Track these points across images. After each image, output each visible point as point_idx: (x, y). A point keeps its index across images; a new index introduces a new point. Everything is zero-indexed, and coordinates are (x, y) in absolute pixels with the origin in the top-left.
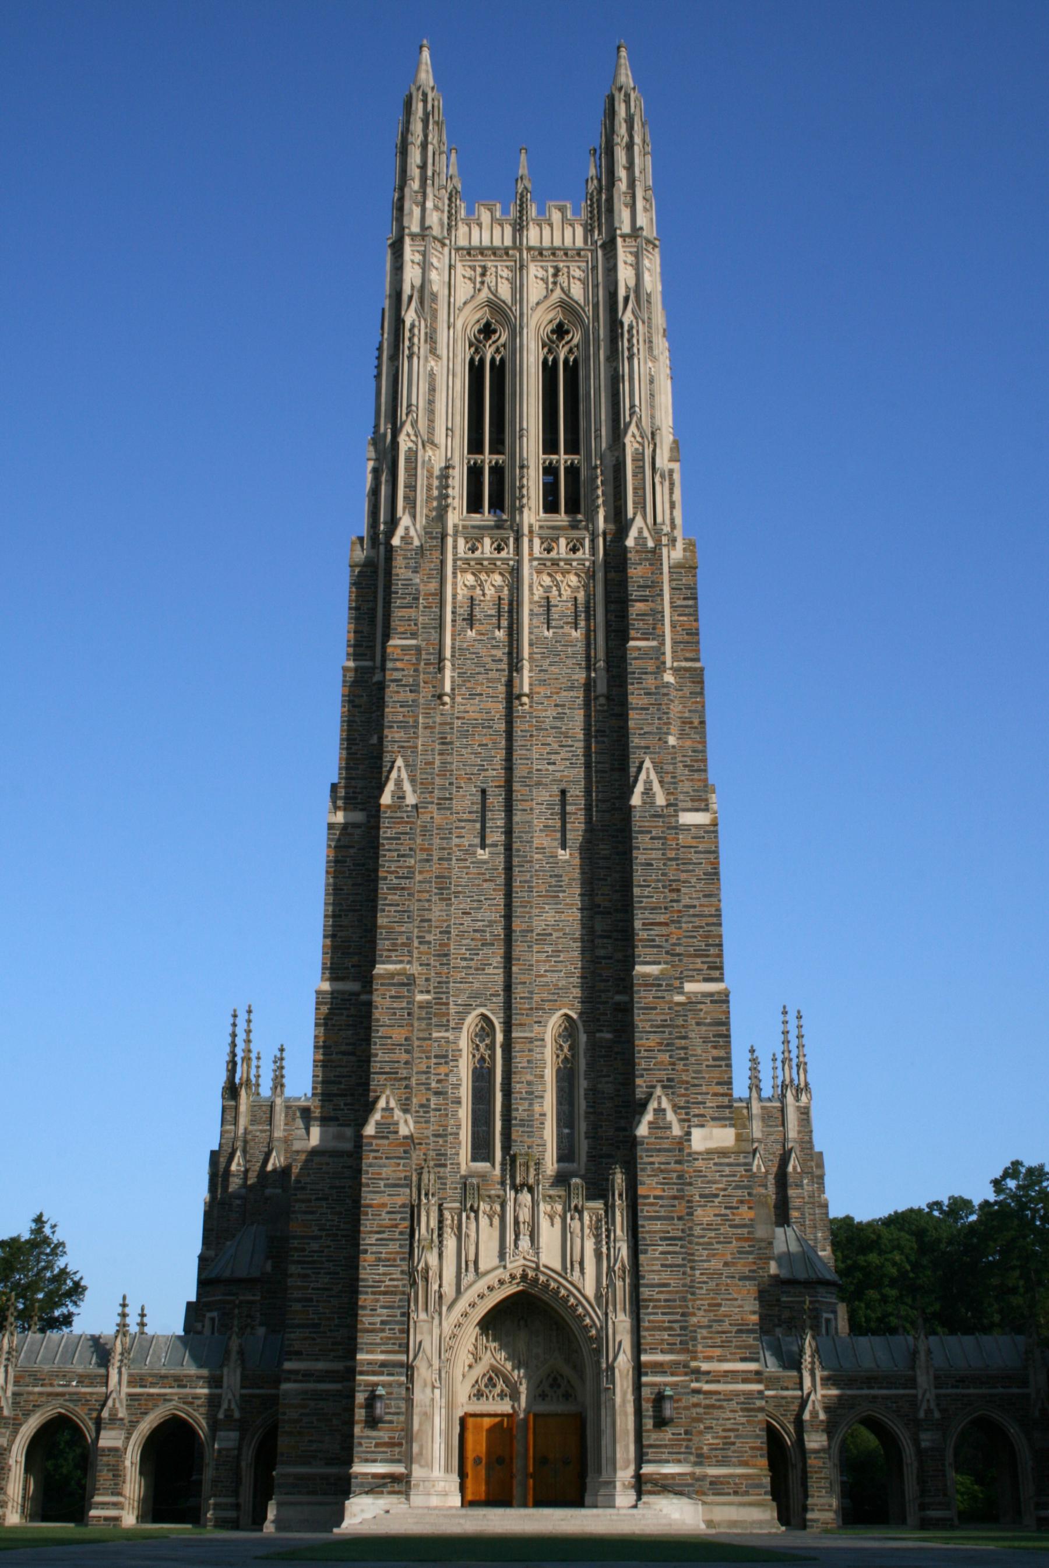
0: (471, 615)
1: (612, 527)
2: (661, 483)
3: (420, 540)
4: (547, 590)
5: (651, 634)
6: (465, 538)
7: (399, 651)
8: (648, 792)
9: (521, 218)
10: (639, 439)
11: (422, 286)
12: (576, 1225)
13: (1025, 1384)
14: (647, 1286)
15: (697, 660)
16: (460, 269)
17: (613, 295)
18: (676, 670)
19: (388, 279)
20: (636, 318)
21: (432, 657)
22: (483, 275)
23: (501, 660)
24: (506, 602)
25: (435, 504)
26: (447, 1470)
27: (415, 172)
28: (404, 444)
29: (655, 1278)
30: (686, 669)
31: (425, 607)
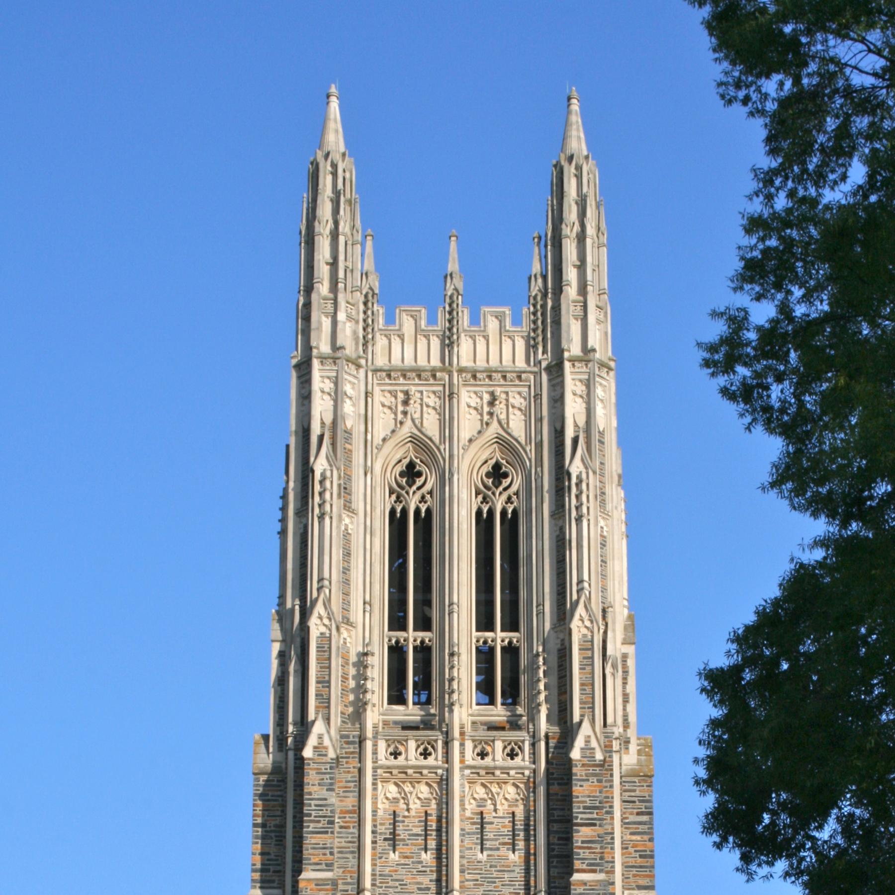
0: (394, 833)
1: (556, 729)
2: (613, 674)
3: (335, 751)
4: (481, 803)
5: (598, 865)
6: (387, 740)
7: (313, 886)
9: (450, 329)
10: (588, 623)
11: (334, 423)
16: (378, 397)
17: (558, 433)
19: (293, 411)
20: (586, 468)
21: (349, 887)
22: (406, 403)
23: (428, 889)
24: (434, 818)
25: (351, 697)
27: (323, 271)
28: (316, 628)
31: (341, 827)
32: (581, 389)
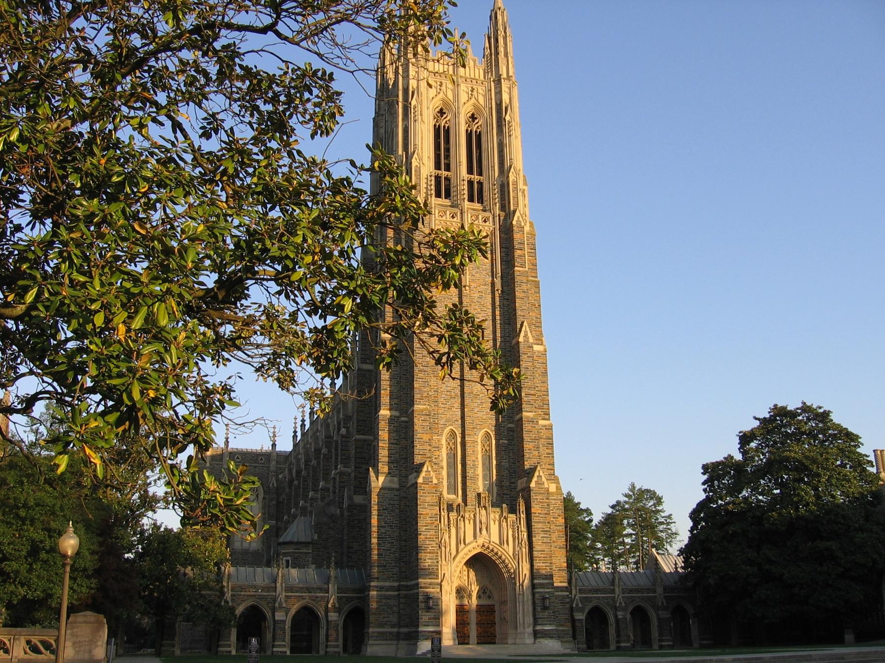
8: (526, 336)
12: (504, 524)
13: (655, 592)
14: (536, 551)
15: (536, 277)
22: (441, 86)
28: (414, 163)
30: (533, 281)
32: (507, 90)
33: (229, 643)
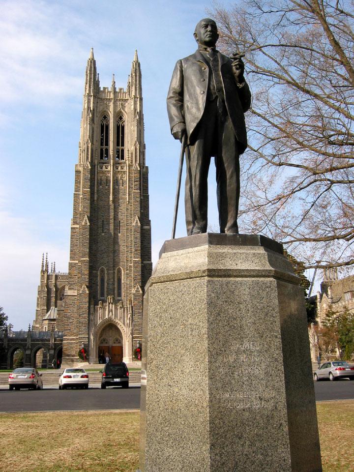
18: (143, 196)
26: (96, 357)
29: (136, 321)
33: (6, 364)
